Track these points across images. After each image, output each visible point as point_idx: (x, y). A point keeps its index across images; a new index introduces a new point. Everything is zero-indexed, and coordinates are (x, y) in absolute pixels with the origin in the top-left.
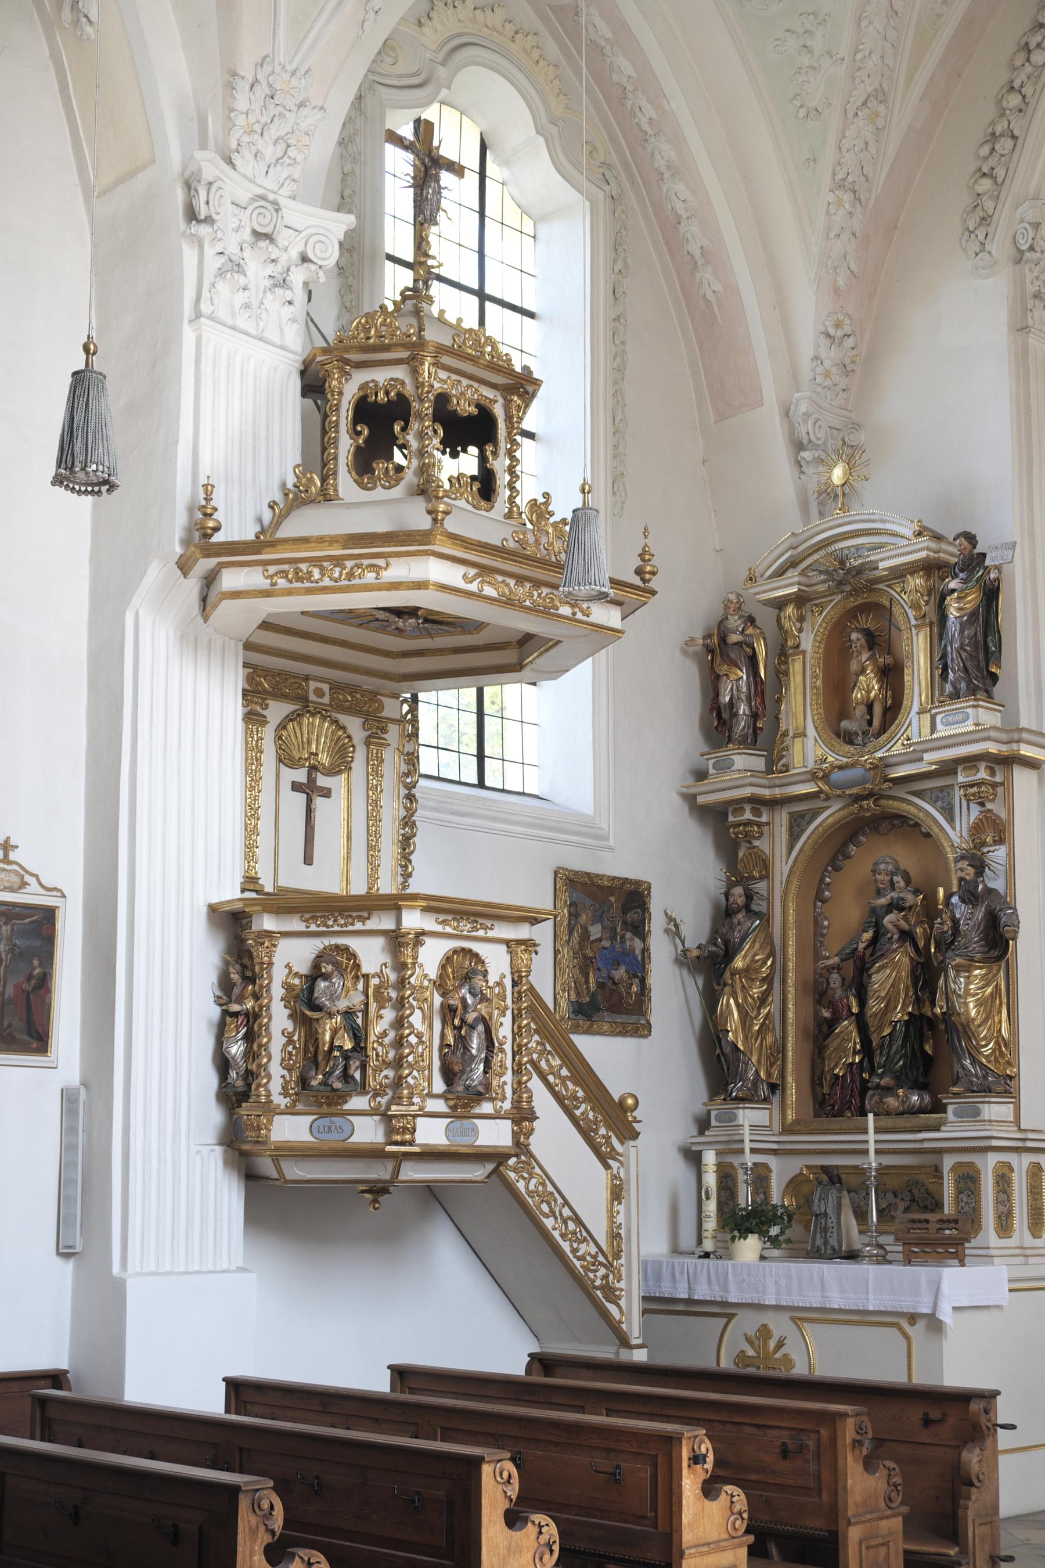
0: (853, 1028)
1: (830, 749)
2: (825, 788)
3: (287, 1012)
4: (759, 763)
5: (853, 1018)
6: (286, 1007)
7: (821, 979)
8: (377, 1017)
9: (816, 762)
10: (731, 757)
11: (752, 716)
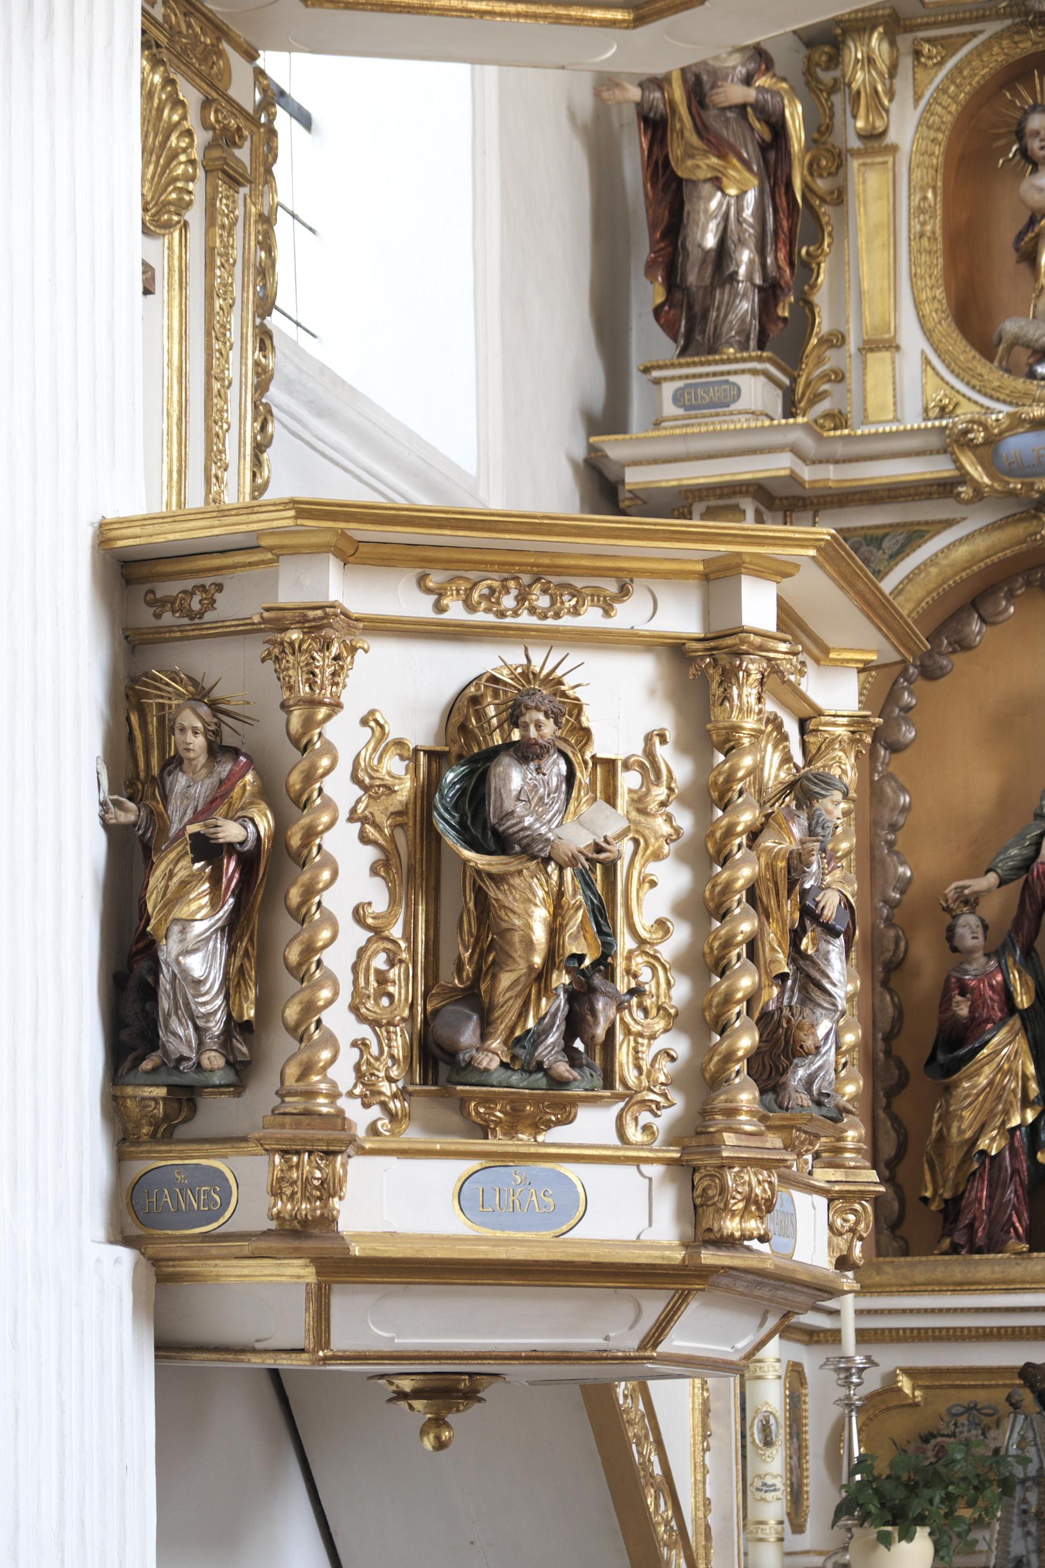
0: (1021, 1044)
1: (968, 384)
2: (976, 472)
3: (370, 854)
4: (775, 402)
5: (1016, 1022)
6: (364, 839)
7: (892, 933)
8: (641, 883)
9: (926, 410)
10: (732, 379)
11: (761, 289)
